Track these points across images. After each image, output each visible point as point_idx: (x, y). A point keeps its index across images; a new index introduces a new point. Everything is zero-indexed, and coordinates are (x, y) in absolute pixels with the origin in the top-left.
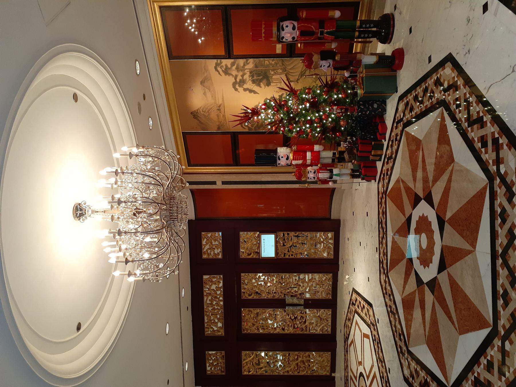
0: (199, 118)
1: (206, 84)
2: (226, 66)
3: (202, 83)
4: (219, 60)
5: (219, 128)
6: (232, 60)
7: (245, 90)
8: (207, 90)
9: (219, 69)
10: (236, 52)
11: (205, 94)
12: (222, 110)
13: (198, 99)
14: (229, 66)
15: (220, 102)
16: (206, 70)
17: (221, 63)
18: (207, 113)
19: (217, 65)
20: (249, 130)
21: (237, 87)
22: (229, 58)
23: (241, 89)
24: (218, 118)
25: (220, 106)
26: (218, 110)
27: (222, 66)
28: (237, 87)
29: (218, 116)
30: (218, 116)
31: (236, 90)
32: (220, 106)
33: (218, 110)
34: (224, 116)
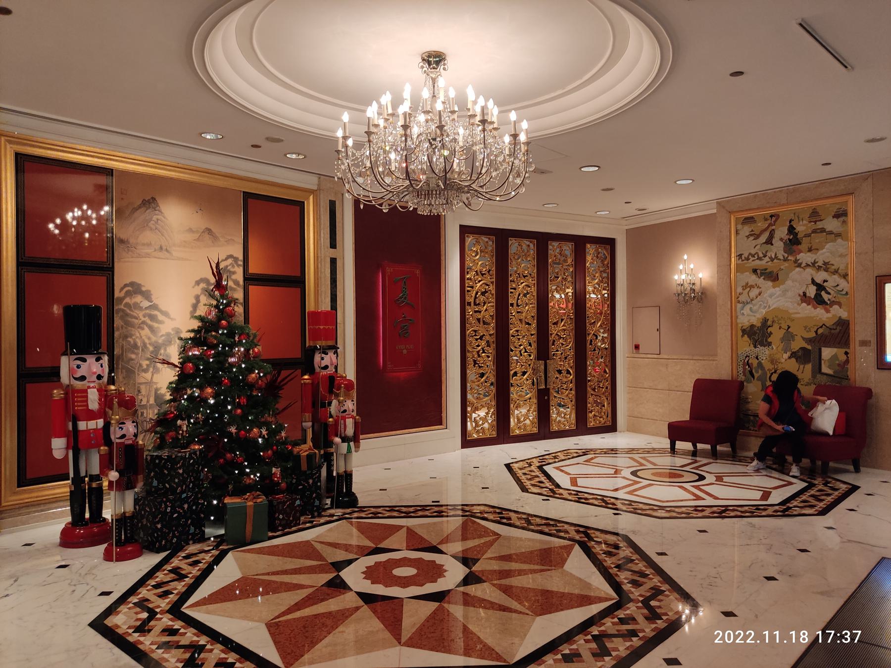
0: (143, 209)
1: (207, 236)
2: (234, 273)
3: (209, 231)
4: (241, 263)
5: (122, 241)
6: (241, 283)
7: (197, 298)
8: (197, 236)
9: (230, 261)
10: (253, 289)
11: (190, 230)
12: (160, 254)
13: (175, 216)
14: (234, 277)
15: (174, 253)
16: (228, 242)
17: (238, 266)
18: (154, 227)
19: (236, 259)
20: (118, 298)
21: (203, 285)
22: (245, 279)
23: (198, 290)
24: (144, 244)
25: (167, 250)
26: (161, 248)
27: (233, 267)
28: (203, 285)
29: (149, 245)
30: (149, 245)
31: (197, 283)
32: (167, 250)
33: (161, 248)
34: (148, 255)
